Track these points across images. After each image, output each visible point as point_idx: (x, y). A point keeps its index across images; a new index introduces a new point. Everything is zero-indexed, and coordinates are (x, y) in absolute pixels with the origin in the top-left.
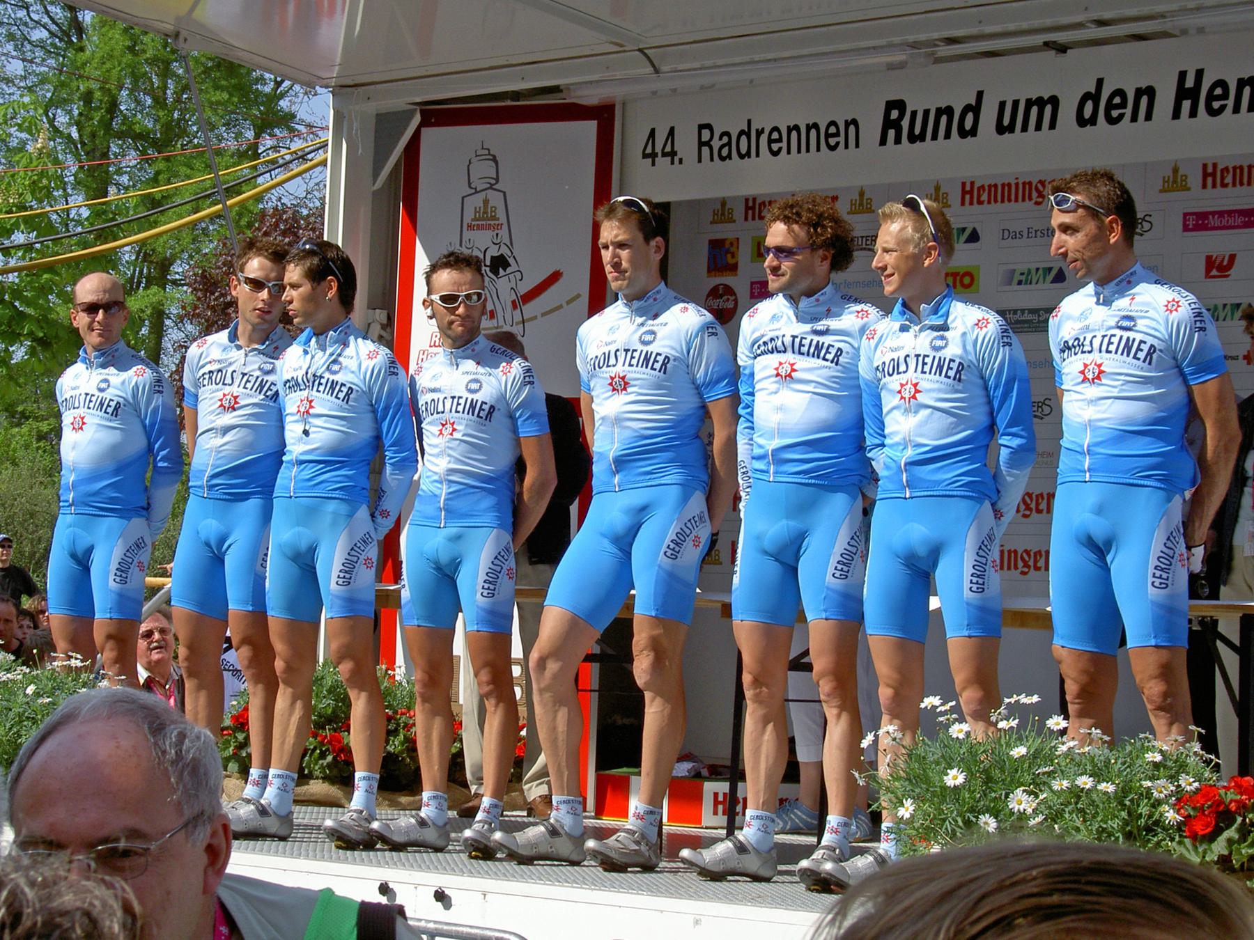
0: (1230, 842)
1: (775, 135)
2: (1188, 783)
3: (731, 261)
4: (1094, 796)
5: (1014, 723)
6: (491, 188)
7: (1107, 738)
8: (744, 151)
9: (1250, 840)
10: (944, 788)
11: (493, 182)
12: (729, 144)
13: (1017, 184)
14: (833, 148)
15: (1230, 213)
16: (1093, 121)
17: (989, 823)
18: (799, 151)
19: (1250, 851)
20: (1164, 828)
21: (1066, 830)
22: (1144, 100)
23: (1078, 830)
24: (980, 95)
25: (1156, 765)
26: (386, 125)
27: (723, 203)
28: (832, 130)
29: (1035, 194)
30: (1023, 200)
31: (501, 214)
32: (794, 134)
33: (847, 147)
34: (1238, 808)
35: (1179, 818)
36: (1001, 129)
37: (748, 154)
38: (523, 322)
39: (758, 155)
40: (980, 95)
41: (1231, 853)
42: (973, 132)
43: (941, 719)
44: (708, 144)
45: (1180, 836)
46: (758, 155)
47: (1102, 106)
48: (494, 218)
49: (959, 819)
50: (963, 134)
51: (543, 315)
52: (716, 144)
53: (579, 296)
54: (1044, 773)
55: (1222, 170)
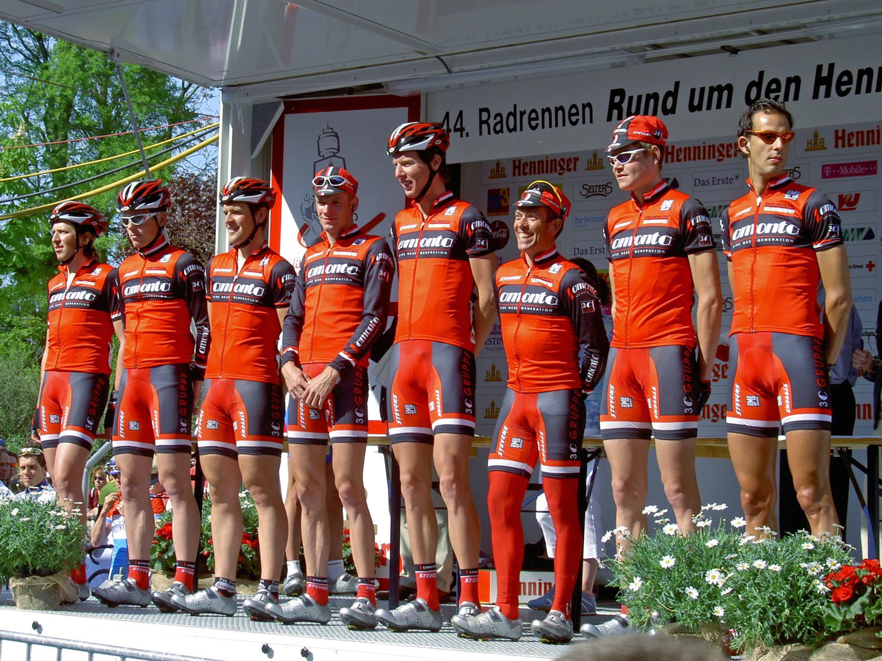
0: (863, 605)
1: (533, 115)
2: (833, 564)
3: (504, 204)
4: (767, 575)
5: (708, 523)
6: (334, 156)
7: (774, 533)
8: (511, 127)
9: (877, 604)
10: (661, 570)
11: (336, 151)
12: (501, 122)
13: (704, 147)
14: (574, 124)
15: (855, 164)
17: (693, 593)
18: (550, 126)
19: (878, 612)
20: (817, 597)
21: (747, 598)
23: (755, 598)
24: (677, 84)
25: (810, 552)
26: (260, 113)
27: (498, 164)
28: (574, 111)
29: (717, 154)
30: (709, 158)
32: (547, 114)
33: (584, 122)
34: (868, 581)
35: (827, 589)
36: (692, 108)
37: (515, 129)
39: (521, 129)
40: (677, 84)
41: (864, 613)
42: (673, 111)
43: (657, 522)
44: (486, 122)
45: (828, 602)
46: (521, 129)
49: (671, 592)
50: (666, 112)
52: (492, 122)
54: (731, 559)
55: (849, 135)
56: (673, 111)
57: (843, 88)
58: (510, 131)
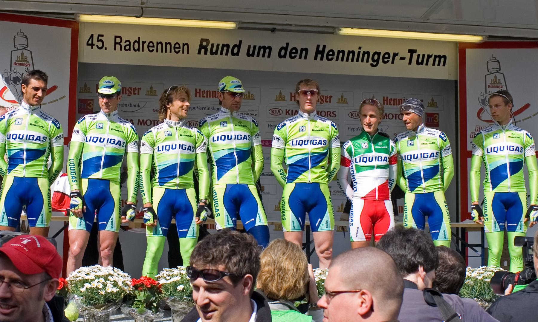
1: (151, 44)
6: (25, 48)
12: (129, 45)
16: (285, 56)
18: (162, 51)
22: (304, 52)
24: (240, 42)
31: (29, 59)
32: (160, 45)
36: (248, 55)
37: (138, 50)
39: (143, 51)
40: (240, 42)
42: (237, 54)
44: (119, 43)
46: (143, 51)
47: (287, 52)
51: (49, 103)
52: (123, 44)
53: (64, 97)
56: (237, 54)
57: (330, 57)
58: (135, 50)
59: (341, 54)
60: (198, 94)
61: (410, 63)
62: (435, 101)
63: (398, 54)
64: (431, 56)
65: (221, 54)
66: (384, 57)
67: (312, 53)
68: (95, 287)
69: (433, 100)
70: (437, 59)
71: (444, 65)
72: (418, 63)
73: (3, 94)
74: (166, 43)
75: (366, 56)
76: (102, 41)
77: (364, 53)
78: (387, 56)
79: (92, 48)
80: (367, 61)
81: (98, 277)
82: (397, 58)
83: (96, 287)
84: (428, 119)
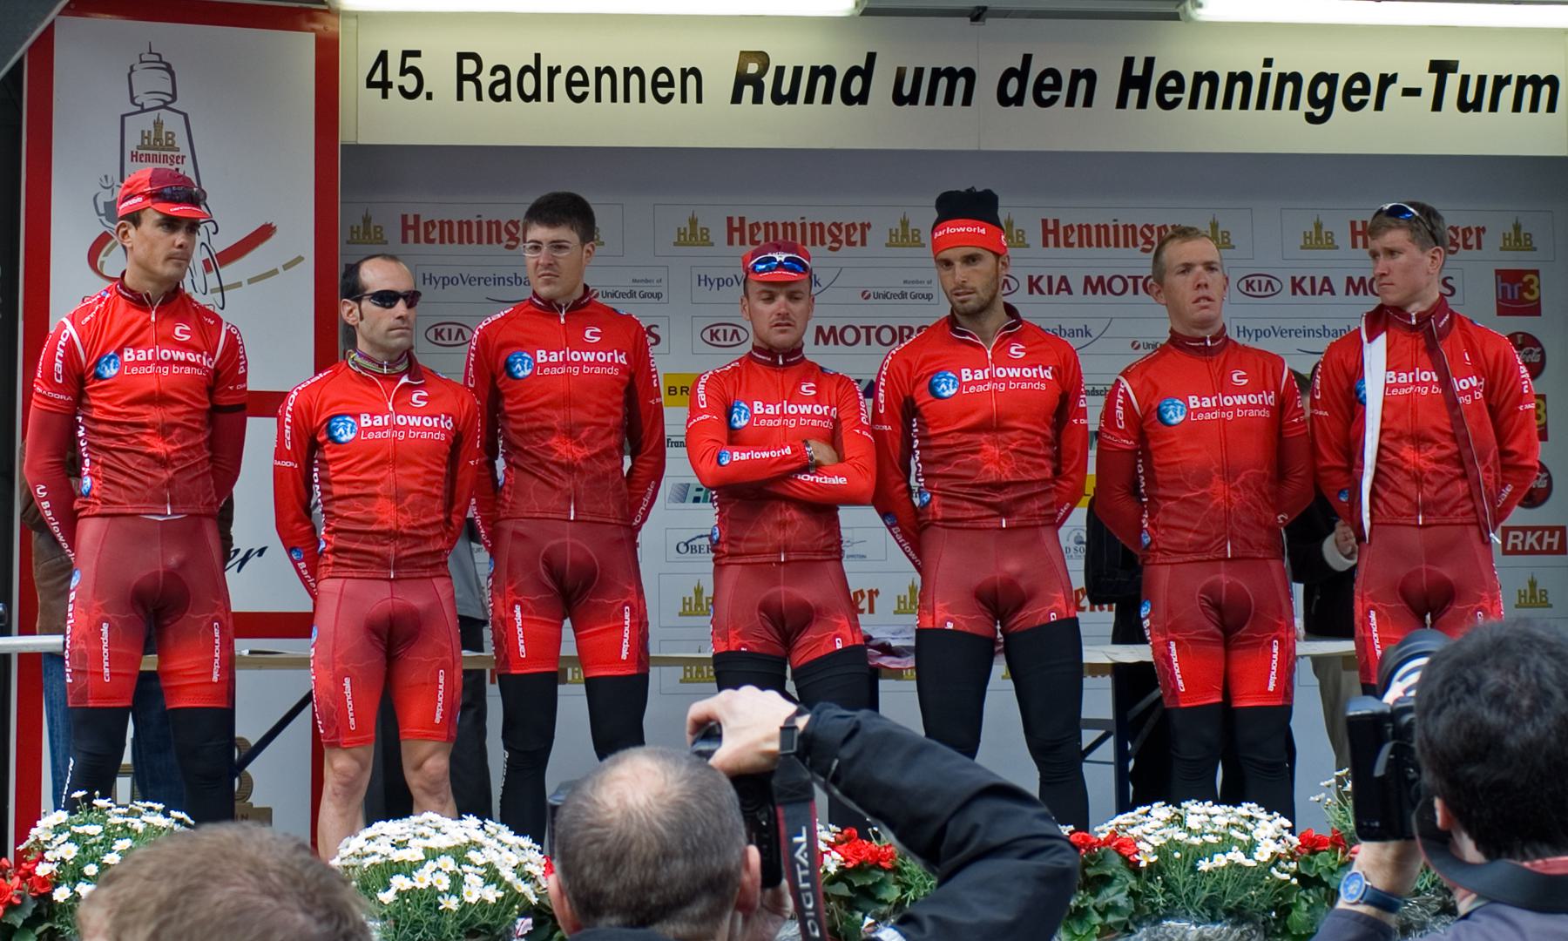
1: (577, 77)
6: (165, 106)
11: (168, 99)
12: (507, 80)
16: (1019, 100)
18: (614, 99)
22: (1083, 84)
24: (871, 57)
31: (181, 141)
32: (606, 79)
36: (899, 99)
37: (536, 96)
38: (222, 289)
39: (551, 98)
40: (871, 57)
42: (863, 98)
46: (551, 98)
47: (1025, 85)
48: (172, 147)
51: (251, 281)
52: (486, 79)
53: (300, 259)
56: (863, 98)
58: (526, 99)
59: (1205, 86)
60: (736, 235)
61: (1437, 105)
62: (1523, 231)
63: (1395, 76)
64: (1508, 80)
65: (809, 99)
66: (1349, 91)
67: (1108, 86)
68: (424, 886)
69: (1517, 228)
70: (1529, 89)
71: (1551, 108)
72: (1463, 106)
73: (101, 258)
74: (626, 69)
75: (1289, 87)
76: (416, 71)
77: (1283, 78)
78: (1358, 85)
79: (385, 96)
80: (1295, 105)
81: (432, 854)
82: (1393, 91)
83: (431, 887)
84: (1504, 289)
